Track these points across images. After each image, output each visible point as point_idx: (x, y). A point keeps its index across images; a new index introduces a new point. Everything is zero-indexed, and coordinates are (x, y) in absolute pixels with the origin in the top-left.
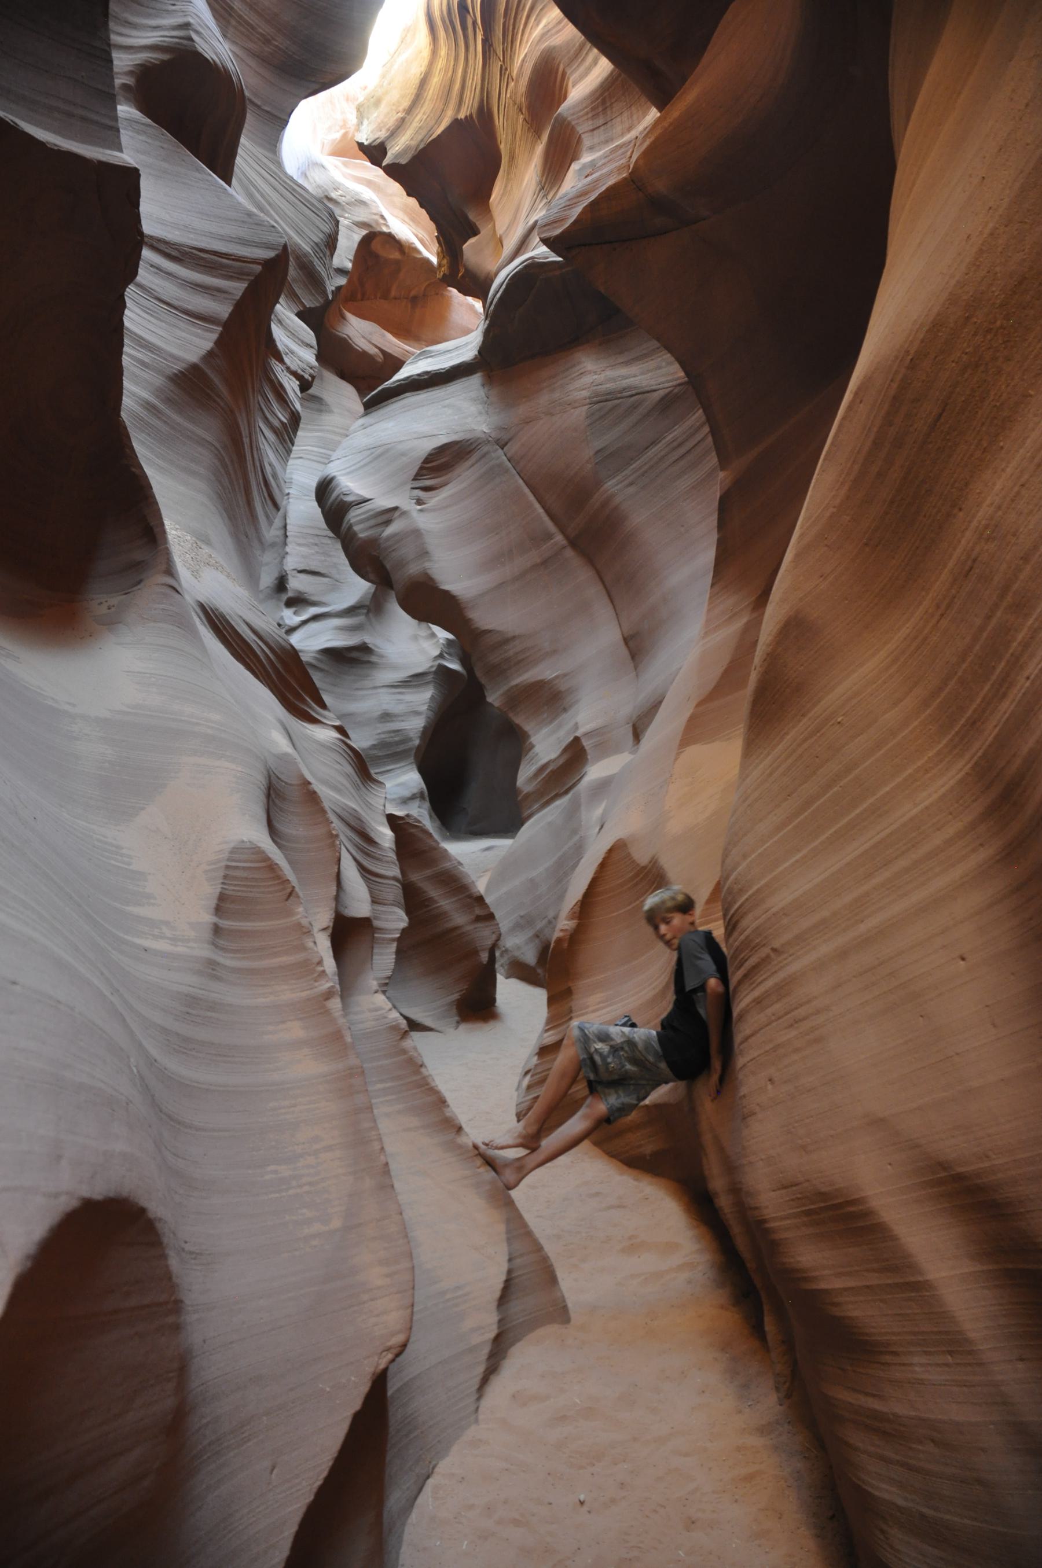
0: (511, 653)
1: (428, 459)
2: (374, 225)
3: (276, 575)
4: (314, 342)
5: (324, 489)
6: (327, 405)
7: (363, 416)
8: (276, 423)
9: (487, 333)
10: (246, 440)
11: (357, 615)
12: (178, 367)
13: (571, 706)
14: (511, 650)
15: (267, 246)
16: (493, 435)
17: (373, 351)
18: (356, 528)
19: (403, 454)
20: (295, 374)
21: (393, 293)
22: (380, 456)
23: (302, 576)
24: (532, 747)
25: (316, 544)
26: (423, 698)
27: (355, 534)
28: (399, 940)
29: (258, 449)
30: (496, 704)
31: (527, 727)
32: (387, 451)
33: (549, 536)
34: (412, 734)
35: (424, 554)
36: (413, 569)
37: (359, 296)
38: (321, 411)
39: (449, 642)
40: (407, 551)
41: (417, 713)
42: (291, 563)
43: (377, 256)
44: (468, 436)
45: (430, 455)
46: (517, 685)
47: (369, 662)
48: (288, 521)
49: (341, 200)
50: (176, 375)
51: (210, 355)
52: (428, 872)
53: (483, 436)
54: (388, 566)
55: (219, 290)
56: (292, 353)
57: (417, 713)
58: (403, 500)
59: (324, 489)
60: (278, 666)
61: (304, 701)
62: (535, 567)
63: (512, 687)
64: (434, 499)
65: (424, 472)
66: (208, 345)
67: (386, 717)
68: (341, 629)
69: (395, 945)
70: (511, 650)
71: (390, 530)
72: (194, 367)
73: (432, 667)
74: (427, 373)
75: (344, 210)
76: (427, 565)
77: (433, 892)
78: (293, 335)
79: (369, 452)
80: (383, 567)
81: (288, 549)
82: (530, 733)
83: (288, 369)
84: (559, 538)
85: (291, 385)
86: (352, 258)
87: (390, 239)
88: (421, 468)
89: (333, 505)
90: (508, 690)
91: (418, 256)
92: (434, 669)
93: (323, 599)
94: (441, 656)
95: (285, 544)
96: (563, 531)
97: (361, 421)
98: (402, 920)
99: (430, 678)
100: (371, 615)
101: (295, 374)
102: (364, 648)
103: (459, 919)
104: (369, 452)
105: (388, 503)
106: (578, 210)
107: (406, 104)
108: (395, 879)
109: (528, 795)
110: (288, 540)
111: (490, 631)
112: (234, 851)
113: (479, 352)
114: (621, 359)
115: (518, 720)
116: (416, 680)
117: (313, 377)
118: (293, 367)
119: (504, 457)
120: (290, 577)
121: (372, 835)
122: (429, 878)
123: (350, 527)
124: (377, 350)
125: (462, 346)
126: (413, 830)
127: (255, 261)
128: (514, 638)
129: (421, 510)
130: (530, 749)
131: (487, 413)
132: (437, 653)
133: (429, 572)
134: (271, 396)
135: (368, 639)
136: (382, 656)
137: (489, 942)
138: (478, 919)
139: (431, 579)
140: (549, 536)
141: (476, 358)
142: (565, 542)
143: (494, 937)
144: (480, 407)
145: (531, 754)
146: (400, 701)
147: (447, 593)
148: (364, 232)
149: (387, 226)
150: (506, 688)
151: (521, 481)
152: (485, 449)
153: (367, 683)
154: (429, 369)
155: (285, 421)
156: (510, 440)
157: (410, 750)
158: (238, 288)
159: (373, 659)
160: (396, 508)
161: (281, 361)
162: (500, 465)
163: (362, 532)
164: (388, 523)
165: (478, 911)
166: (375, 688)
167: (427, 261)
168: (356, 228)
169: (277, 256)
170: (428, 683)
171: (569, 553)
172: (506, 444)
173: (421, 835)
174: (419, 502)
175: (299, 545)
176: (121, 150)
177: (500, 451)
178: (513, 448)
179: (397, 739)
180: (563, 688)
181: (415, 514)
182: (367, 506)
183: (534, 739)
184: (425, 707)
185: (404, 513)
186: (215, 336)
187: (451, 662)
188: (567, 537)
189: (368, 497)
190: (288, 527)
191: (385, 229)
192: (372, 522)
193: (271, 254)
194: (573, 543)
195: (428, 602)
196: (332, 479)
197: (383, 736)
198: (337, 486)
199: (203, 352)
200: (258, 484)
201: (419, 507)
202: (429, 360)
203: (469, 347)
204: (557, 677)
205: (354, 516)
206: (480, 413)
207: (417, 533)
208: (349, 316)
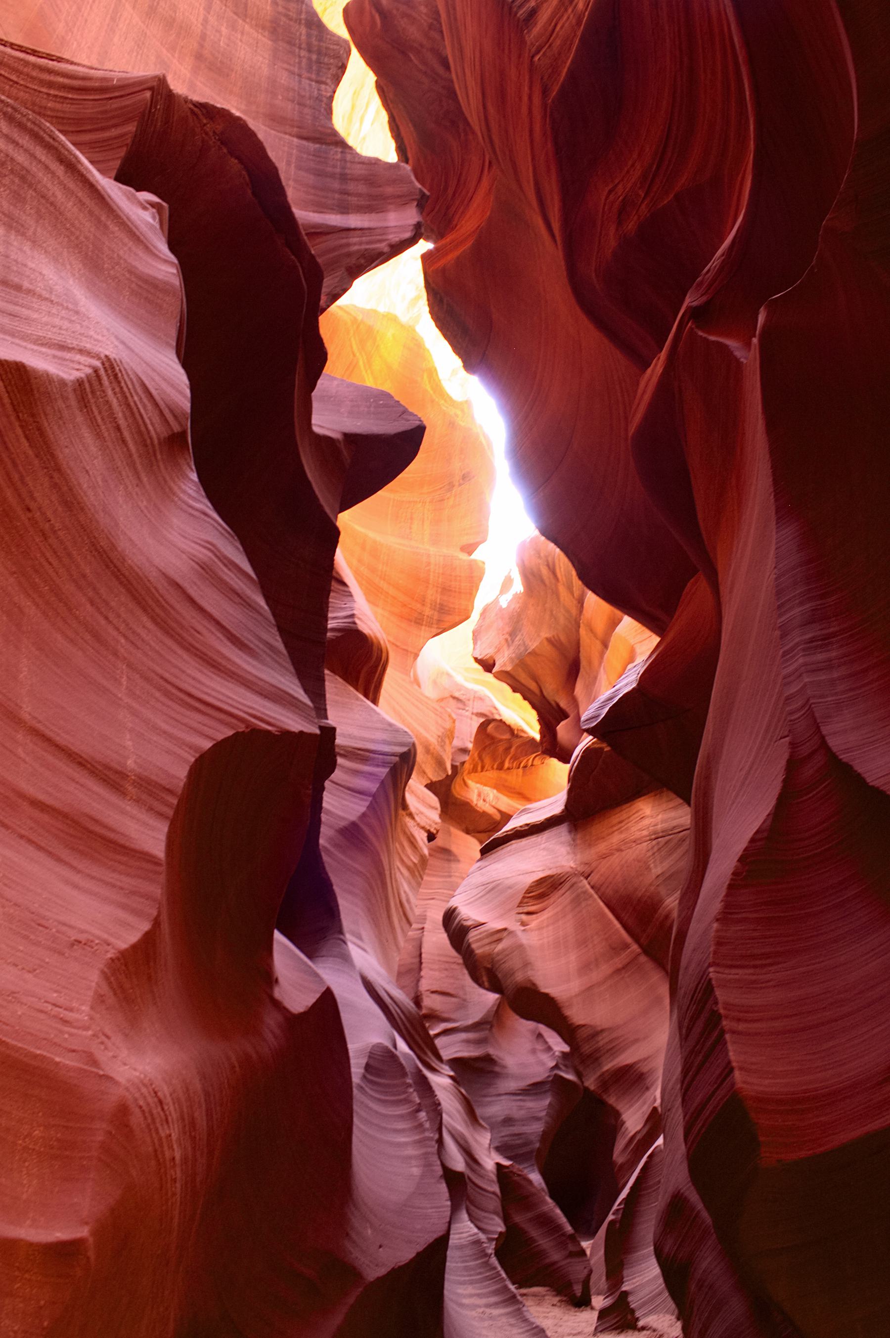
0: (601, 1043)
1: (528, 891)
2: (488, 714)
3: (413, 995)
4: (438, 805)
5: (450, 916)
6: (455, 856)
7: (479, 861)
8: (410, 864)
9: (570, 792)
10: (387, 873)
11: (483, 1030)
12: (343, 824)
13: (652, 1085)
14: (602, 1040)
15: (402, 745)
16: (579, 869)
17: (491, 811)
18: (474, 946)
19: (510, 887)
20: (423, 828)
21: (506, 765)
22: (492, 889)
23: (435, 996)
24: (623, 1123)
25: (446, 970)
26: (541, 1105)
27: (472, 951)
28: (497, 1239)
29: (396, 881)
30: (592, 1088)
31: (619, 1107)
32: (498, 885)
33: (626, 946)
34: (532, 1138)
35: (526, 964)
36: (519, 977)
37: (479, 768)
38: (449, 861)
39: (564, 1055)
40: (515, 962)
41: (538, 1119)
42: (425, 985)
43: (492, 738)
44: (559, 871)
45: (531, 887)
46: (607, 1071)
47: (492, 1072)
48: (423, 950)
49: (462, 697)
50: (341, 829)
51: (364, 815)
52: (529, 1215)
53: (569, 870)
54: (500, 975)
55: (371, 774)
56: (422, 813)
57: (538, 1119)
58: (510, 923)
59: (450, 916)
60: (406, 1022)
61: (425, 1054)
62: (618, 971)
63: (603, 1074)
64: (534, 922)
65: (526, 900)
66: (363, 809)
67: (508, 1121)
68: (468, 1041)
69: (494, 1243)
70: (602, 1040)
71: (500, 947)
72: (354, 824)
73: (549, 1076)
74: (527, 825)
75: (464, 704)
76: (530, 973)
77: (534, 1233)
78: (423, 802)
79: (483, 887)
80: (496, 976)
81: (422, 973)
82: (622, 1111)
83: (418, 824)
84: (635, 947)
85: (421, 837)
86: (472, 740)
87: (502, 724)
88: (524, 897)
89: (456, 929)
90: (600, 1076)
91: (525, 735)
92: (551, 1079)
93: (452, 1016)
94: (556, 1067)
95: (420, 969)
96: (637, 940)
97: (479, 864)
98: (499, 1225)
99: (547, 1087)
100: (494, 1030)
101: (423, 828)
102: (488, 1059)
103: (555, 1256)
104: (483, 887)
105: (499, 925)
106: (606, 709)
107: (508, 629)
108: (494, 1193)
109: (622, 1165)
110: (423, 965)
111: (584, 1026)
112: (373, 1046)
113: (566, 806)
114: (664, 806)
115: (612, 1100)
116: (534, 1089)
117: (438, 831)
118: (423, 824)
119: (588, 887)
120: (424, 997)
121: (477, 1157)
122: (530, 1220)
123: (469, 945)
124: (495, 811)
125: (554, 803)
126: (516, 1178)
127: (393, 755)
128: (602, 1031)
129: (524, 930)
130: (622, 1125)
131: (574, 853)
132: (552, 1064)
133: (531, 978)
134: (406, 844)
135: (491, 1051)
136: (504, 1067)
137: (583, 1275)
138: (571, 1255)
139: (534, 984)
140: (626, 946)
141: (562, 812)
142: (639, 950)
143: (586, 1272)
144: (568, 848)
145: (623, 1129)
146: (521, 1108)
147: (547, 995)
148: (482, 720)
149: (500, 715)
150: (598, 1074)
151: (602, 904)
152: (574, 880)
153: (492, 1091)
154: (528, 822)
155: (416, 861)
156: (592, 872)
157: (531, 1152)
158: (383, 771)
159: (497, 1069)
160: (505, 929)
161: (413, 818)
162: (585, 892)
163: (479, 949)
164: (499, 940)
165: (571, 1247)
166: (500, 1095)
167: (533, 739)
168: (474, 717)
169: (409, 750)
170: (546, 1092)
171: (643, 959)
172: (589, 875)
173: (523, 1182)
174: (523, 924)
175: (431, 969)
176: (327, 718)
177: (585, 882)
178: (594, 878)
179: (518, 1142)
180: (645, 1069)
181: (519, 933)
182: (482, 929)
183: (624, 1117)
184: (544, 1113)
185: (511, 932)
186: (367, 804)
187: (567, 1073)
188: (640, 946)
189: (483, 921)
190: (423, 955)
191: (497, 717)
192: (487, 941)
193: (405, 749)
194: (646, 951)
195: (532, 1003)
196: (455, 909)
197: (506, 1139)
198: (458, 914)
199: (359, 814)
200: (396, 905)
201: (523, 928)
202: (529, 815)
203: (559, 803)
204: (640, 1061)
205: (472, 936)
206: (568, 853)
207: (520, 947)
208: (470, 783)
